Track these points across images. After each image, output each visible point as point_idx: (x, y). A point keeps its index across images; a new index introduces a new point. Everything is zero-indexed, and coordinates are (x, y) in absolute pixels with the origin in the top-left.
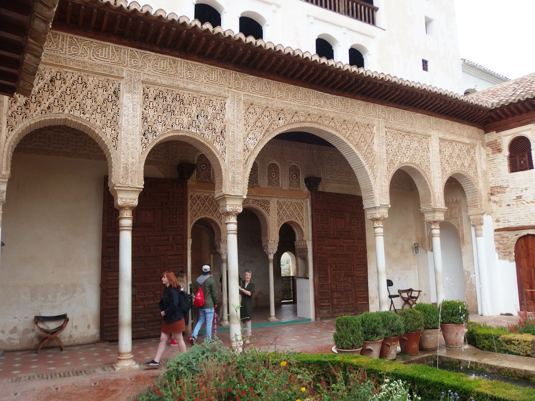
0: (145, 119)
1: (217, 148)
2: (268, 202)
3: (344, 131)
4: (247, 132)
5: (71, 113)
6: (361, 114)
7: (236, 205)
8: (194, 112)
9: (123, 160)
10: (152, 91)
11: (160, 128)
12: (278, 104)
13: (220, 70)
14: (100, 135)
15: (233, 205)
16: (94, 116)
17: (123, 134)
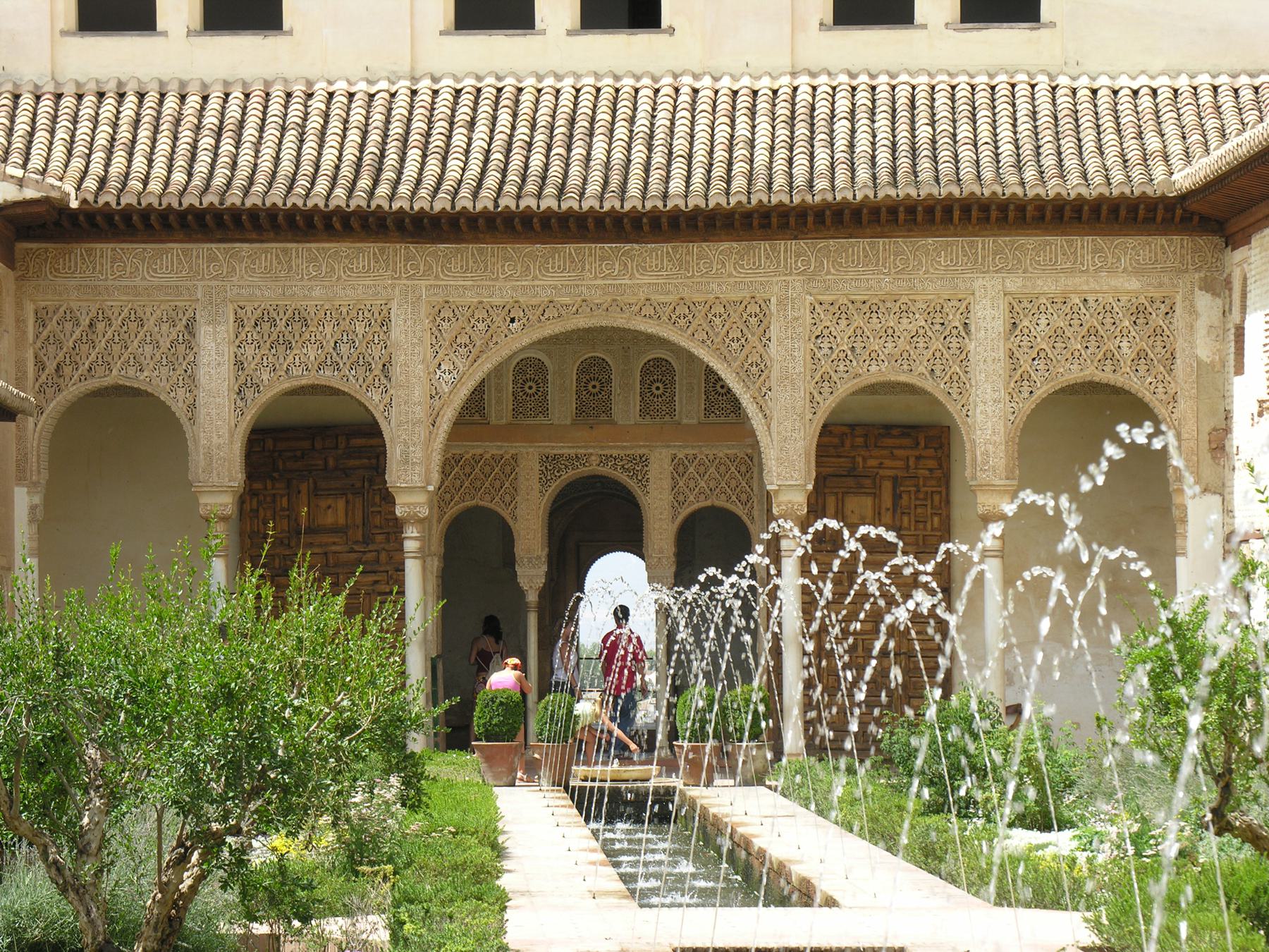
0: (239, 364)
1: (373, 400)
2: (644, 460)
3: (682, 322)
4: (436, 361)
5: (123, 373)
6: (730, 275)
7: (415, 505)
8: (329, 336)
9: (203, 442)
10: (249, 313)
11: (265, 377)
13: (373, 247)
14: (168, 403)
15: (408, 505)
16: (156, 373)
17: (202, 397)
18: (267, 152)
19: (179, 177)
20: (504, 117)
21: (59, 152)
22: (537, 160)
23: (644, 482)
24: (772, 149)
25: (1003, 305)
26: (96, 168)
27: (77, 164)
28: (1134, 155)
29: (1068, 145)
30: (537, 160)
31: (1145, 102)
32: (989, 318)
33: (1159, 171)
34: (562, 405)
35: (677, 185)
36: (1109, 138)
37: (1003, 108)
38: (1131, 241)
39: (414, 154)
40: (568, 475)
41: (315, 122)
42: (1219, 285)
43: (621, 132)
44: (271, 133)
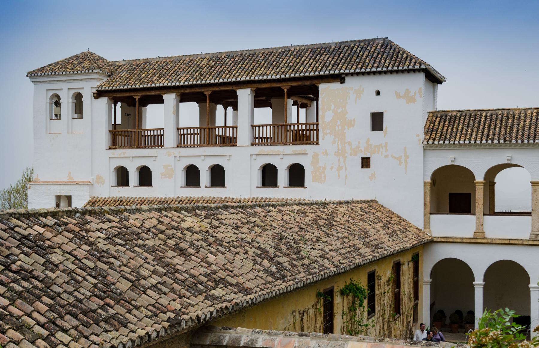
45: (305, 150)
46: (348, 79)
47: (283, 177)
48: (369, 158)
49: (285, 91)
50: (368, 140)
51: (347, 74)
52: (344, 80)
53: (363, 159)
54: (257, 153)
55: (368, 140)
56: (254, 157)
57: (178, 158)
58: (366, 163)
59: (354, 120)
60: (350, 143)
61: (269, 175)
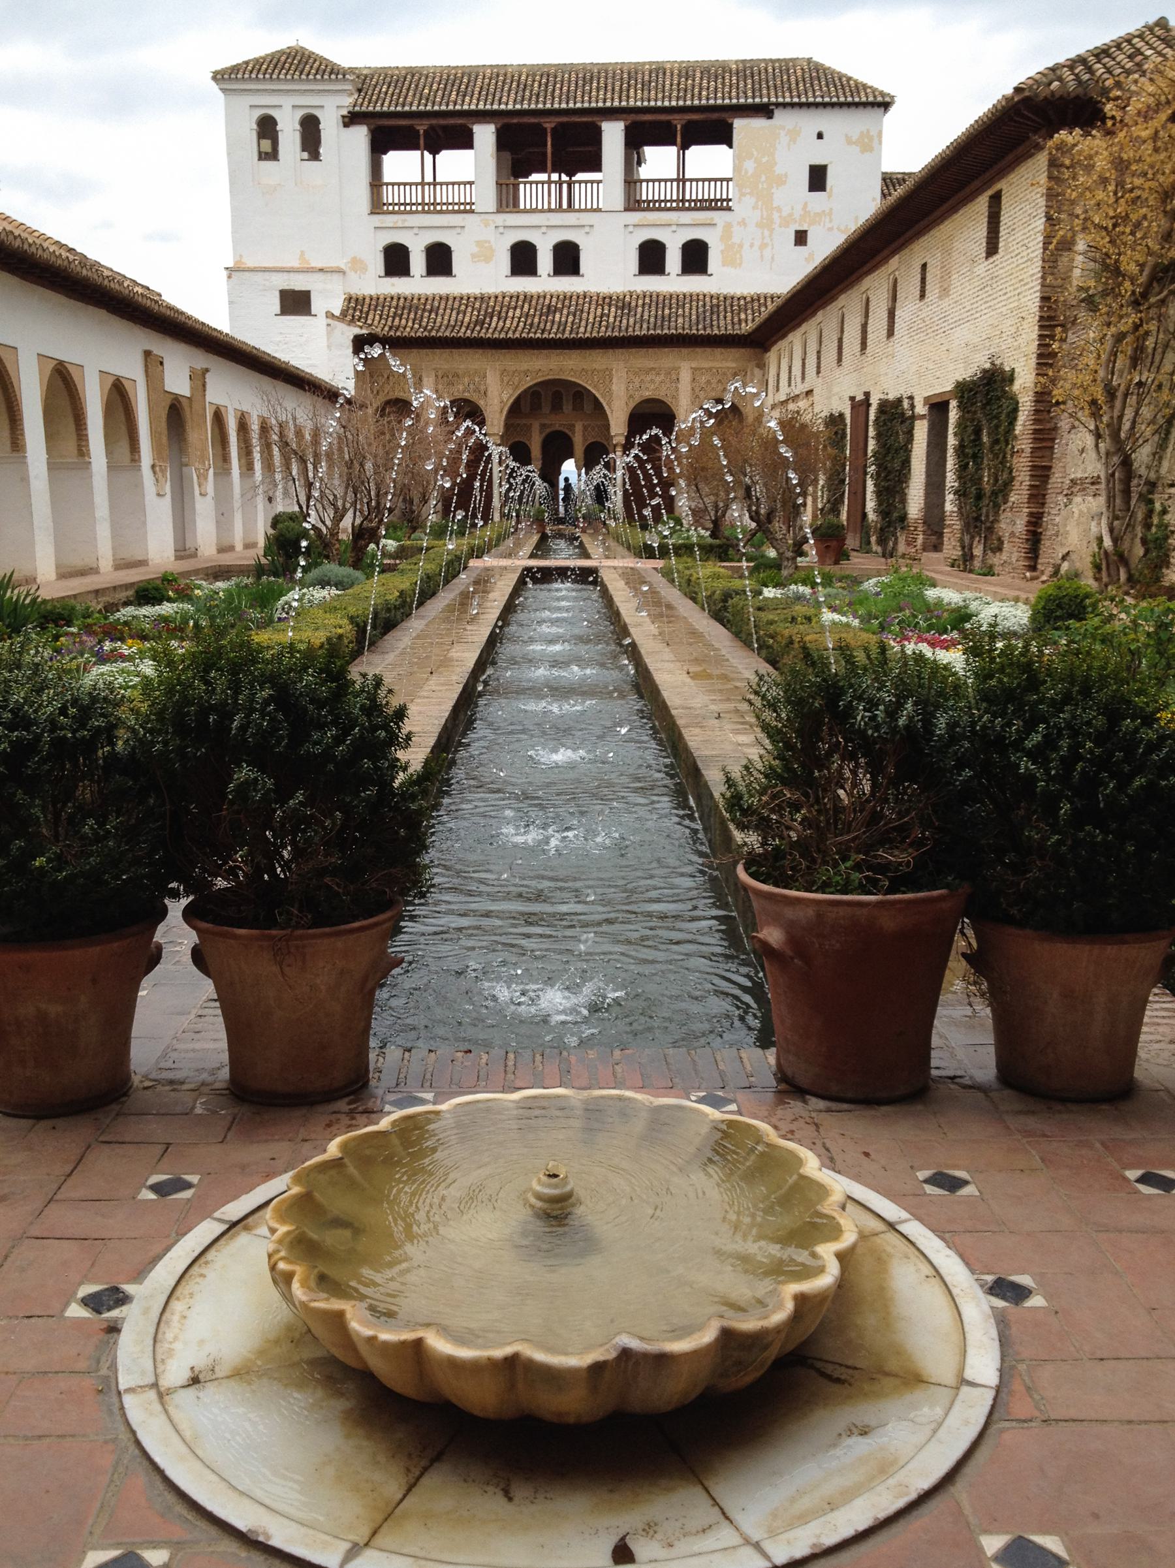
1: (481, 403)
2: (574, 426)
12: (525, 366)
13: (480, 351)
18: (446, 317)
19: (416, 326)
20: (526, 306)
21: (377, 317)
22: (536, 320)
23: (574, 433)
24: (615, 317)
25: (690, 371)
26: (389, 323)
27: (383, 322)
28: (736, 319)
29: (715, 317)
30: (536, 320)
31: (742, 302)
32: (685, 376)
33: (743, 325)
34: (546, 409)
35: (582, 329)
36: (729, 314)
37: (694, 303)
38: (733, 350)
39: (495, 319)
40: (548, 431)
41: (463, 307)
42: (762, 366)
43: (565, 312)
44: (448, 311)
45: (712, 219)
46: (776, 112)
47: (673, 260)
48: (806, 232)
49: (679, 127)
50: (806, 204)
51: (778, 105)
52: (772, 112)
53: (797, 232)
54: (636, 222)
55: (806, 204)
56: (631, 229)
57: (501, 230)
58: (801, 238)
59: (786, 175)
60: (779, 210)
61: (651, 258)
